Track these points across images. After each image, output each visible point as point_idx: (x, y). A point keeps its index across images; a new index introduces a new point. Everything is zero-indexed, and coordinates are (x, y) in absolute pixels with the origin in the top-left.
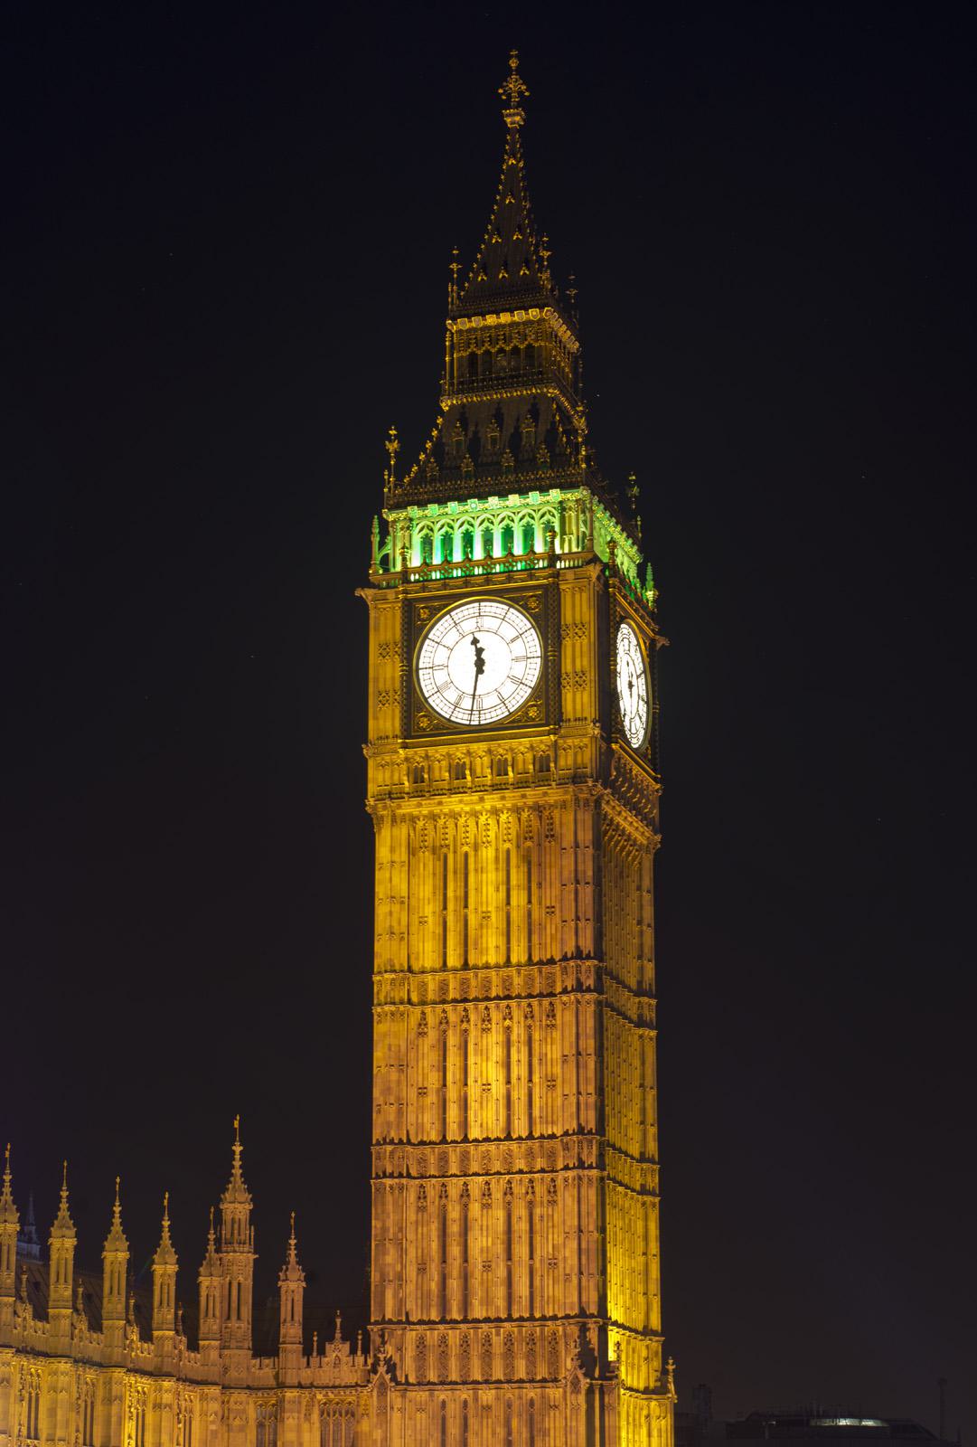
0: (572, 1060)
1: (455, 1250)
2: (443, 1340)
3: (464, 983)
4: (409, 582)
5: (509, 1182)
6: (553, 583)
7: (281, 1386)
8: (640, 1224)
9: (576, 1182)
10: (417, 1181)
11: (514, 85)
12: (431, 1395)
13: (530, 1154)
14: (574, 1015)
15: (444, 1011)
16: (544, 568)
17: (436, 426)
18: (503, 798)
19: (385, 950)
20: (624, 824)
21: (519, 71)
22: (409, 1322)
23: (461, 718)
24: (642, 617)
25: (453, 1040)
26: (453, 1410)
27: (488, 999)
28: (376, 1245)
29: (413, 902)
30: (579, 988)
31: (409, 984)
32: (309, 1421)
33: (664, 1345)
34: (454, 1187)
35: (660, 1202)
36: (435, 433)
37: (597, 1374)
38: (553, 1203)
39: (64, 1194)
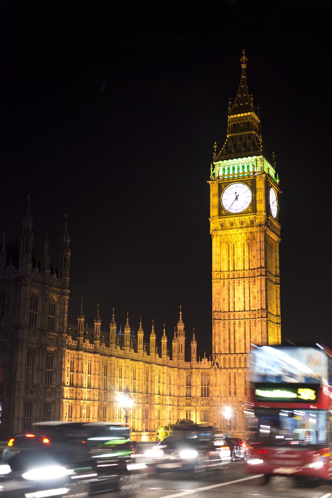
0: (260, 292)
1: (232, 337)
2: (230, 358)
3: (234, 274)
4: (220, 179)
5: (245, 321)
7: (192, 368)
8: (276, 331)
11: (244, 58)
13: (250, 314)
17: (226, 141)
18: (243, 230)
19: (215, 266)
20: (272, 236)
21: (245, 55)
22: (221, 354)
23: (232, 211)
24: (276, 186)
25: (231, 288)
26: (232, 374)
27: (239, 278)
30: (261, 275)
34: (232, 322)
36: (225, 143)
39: (141, 324)
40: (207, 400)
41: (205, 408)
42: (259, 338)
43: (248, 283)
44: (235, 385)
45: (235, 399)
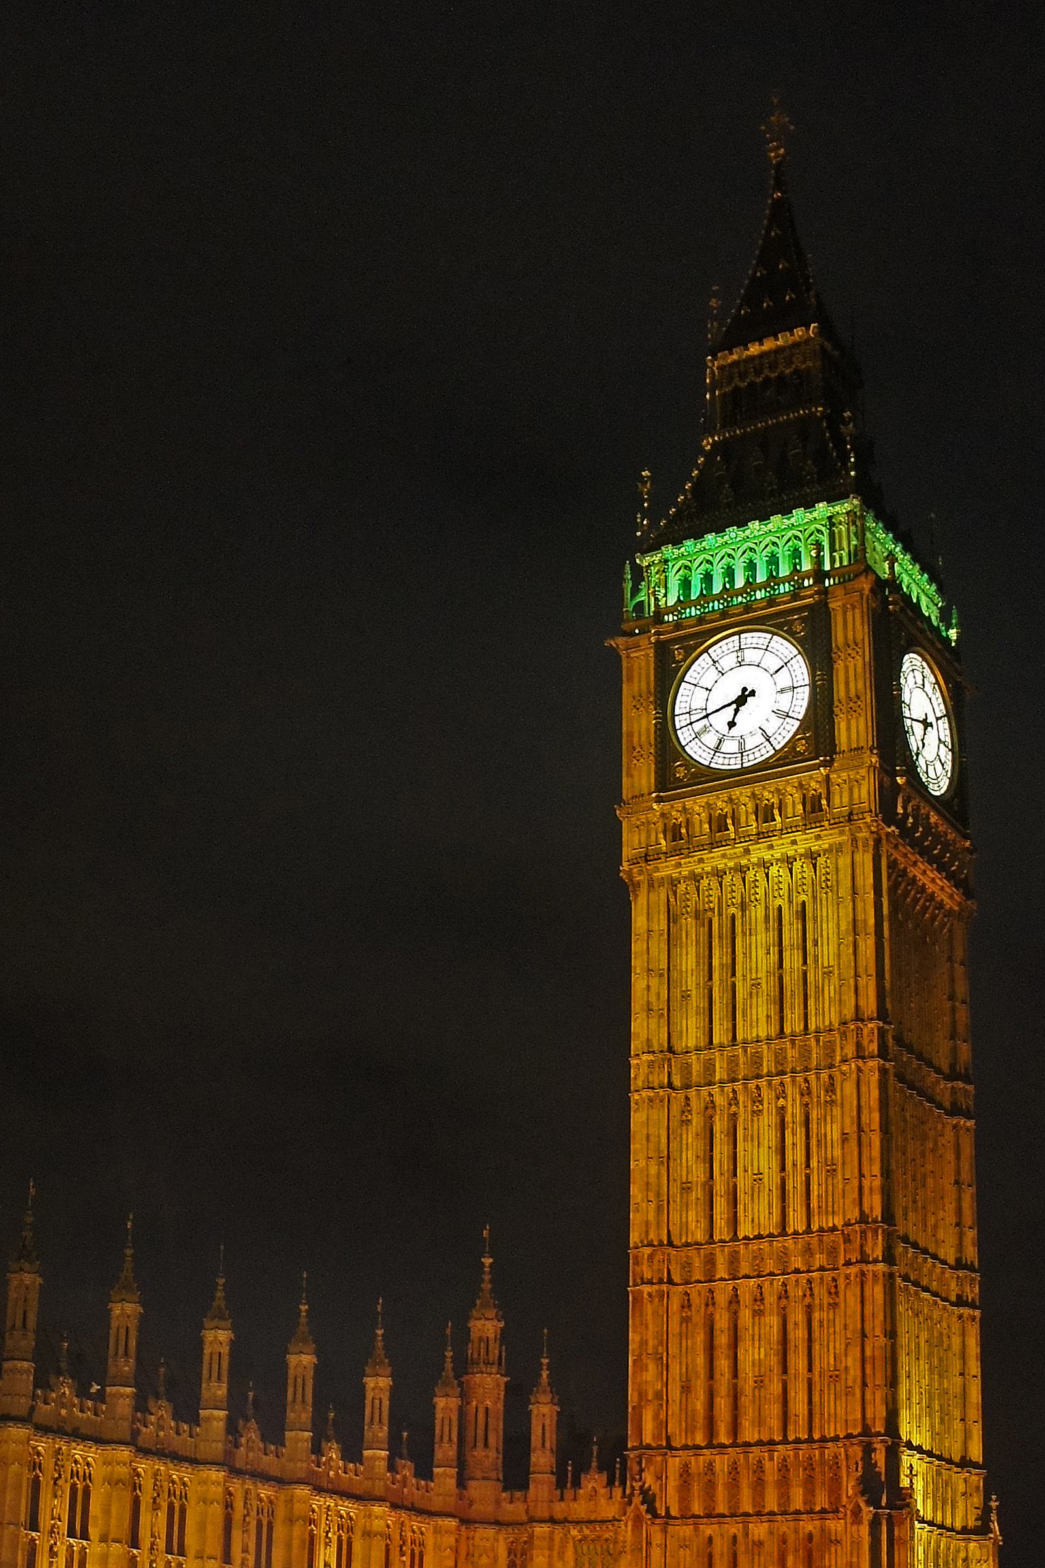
1: (723, 1364)
2: (710, 1466)
3: (733, 1062)
5: (784, 1284)
6: (821, 601)
10: (680, 1288)
13: (808, 1251)
14: (855, 1086)
15: (711, 1095)
16: (810, 586)
18: (771, 847)
20: (923, 880)
23: (719, 763)
25: (719, 1126)
28: (634, 1361)
29: (674, 974)
31: (670, 1066)
38: (834, 1306)
42: (850, 1362)
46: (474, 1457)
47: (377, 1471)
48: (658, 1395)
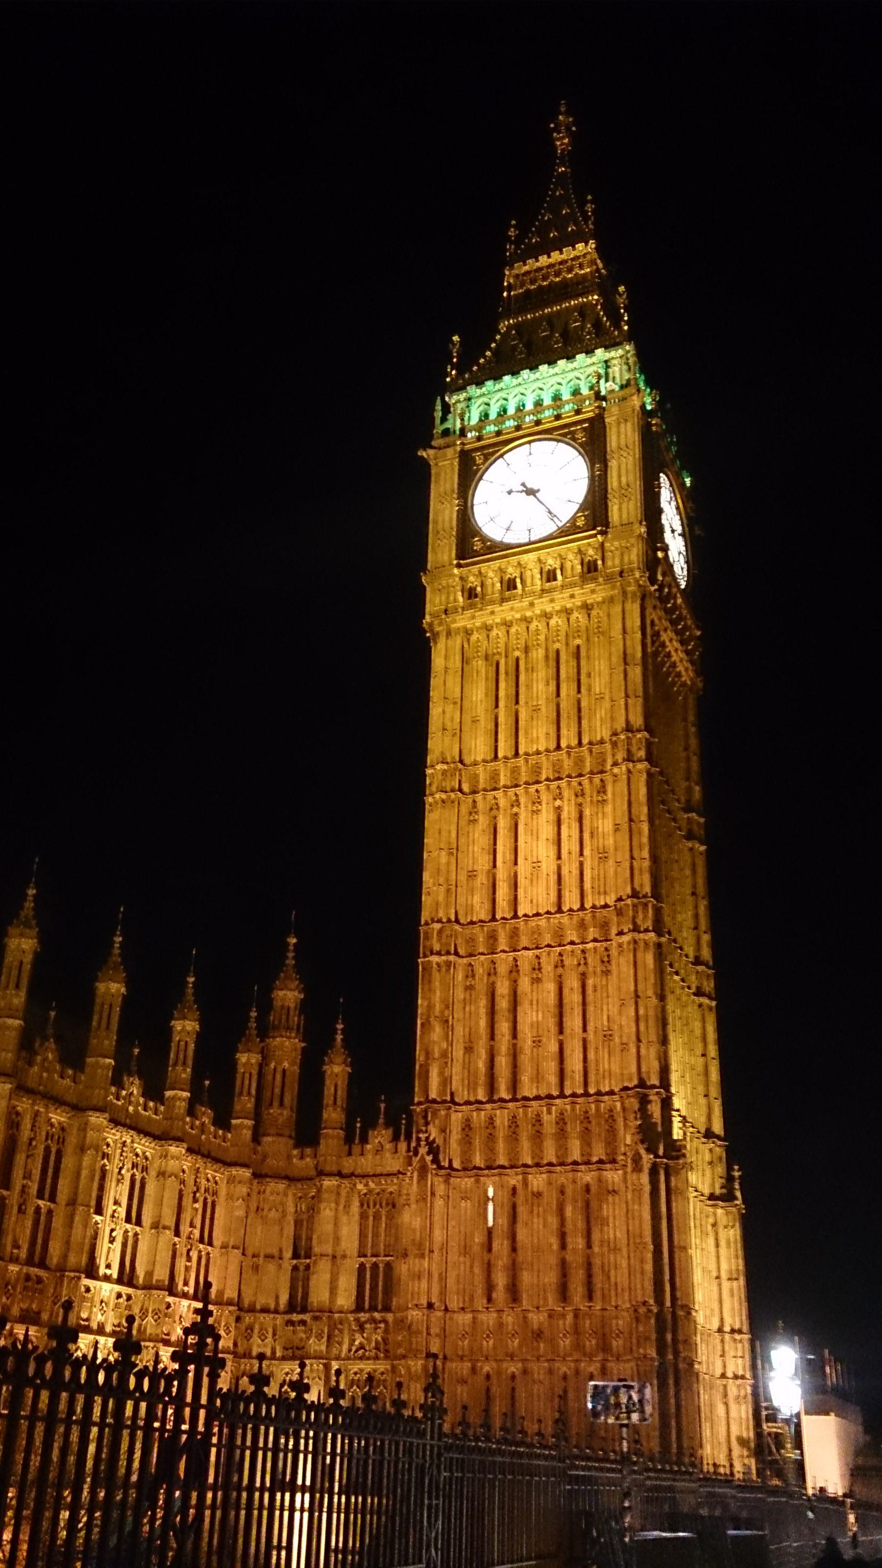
0: (625, 826)
1: (503, 1027)
2: (491, 1120)
3: (515, 771)
5: (560, 954)
7: (321, 1173)
8: (697, 1025)
9: (631, 946)
10: (465, 961)
12: (477, 1181)
13: (582, 926)
18: (552, 601)
23: (510, 539)
25: (503, 824)
28: (422, 1024)
29: (465, 703)
31: (460, 775)
32: (348, 1213)
33: (728, 1150)
34: (503, 962)
35: (717, 1005)
37: (661, 1152)
38: (607, 973)
40: (382, 1325)
41: (367, 1367)
43: (573, 797)
44: (514, 1249)
45: (510, 1319)
46: (269, 1114)
47: (177, 1111)
48: (444, 1054)
